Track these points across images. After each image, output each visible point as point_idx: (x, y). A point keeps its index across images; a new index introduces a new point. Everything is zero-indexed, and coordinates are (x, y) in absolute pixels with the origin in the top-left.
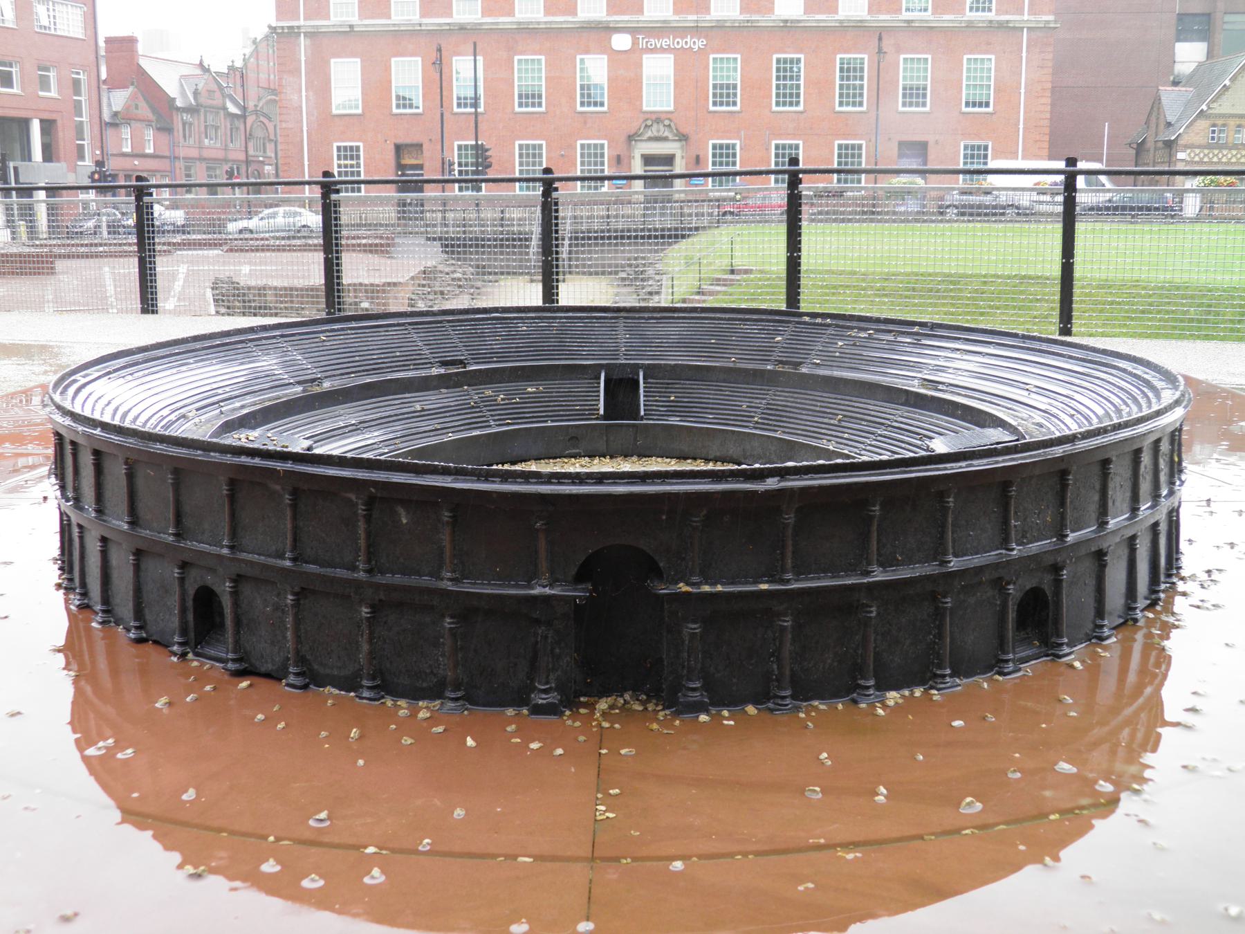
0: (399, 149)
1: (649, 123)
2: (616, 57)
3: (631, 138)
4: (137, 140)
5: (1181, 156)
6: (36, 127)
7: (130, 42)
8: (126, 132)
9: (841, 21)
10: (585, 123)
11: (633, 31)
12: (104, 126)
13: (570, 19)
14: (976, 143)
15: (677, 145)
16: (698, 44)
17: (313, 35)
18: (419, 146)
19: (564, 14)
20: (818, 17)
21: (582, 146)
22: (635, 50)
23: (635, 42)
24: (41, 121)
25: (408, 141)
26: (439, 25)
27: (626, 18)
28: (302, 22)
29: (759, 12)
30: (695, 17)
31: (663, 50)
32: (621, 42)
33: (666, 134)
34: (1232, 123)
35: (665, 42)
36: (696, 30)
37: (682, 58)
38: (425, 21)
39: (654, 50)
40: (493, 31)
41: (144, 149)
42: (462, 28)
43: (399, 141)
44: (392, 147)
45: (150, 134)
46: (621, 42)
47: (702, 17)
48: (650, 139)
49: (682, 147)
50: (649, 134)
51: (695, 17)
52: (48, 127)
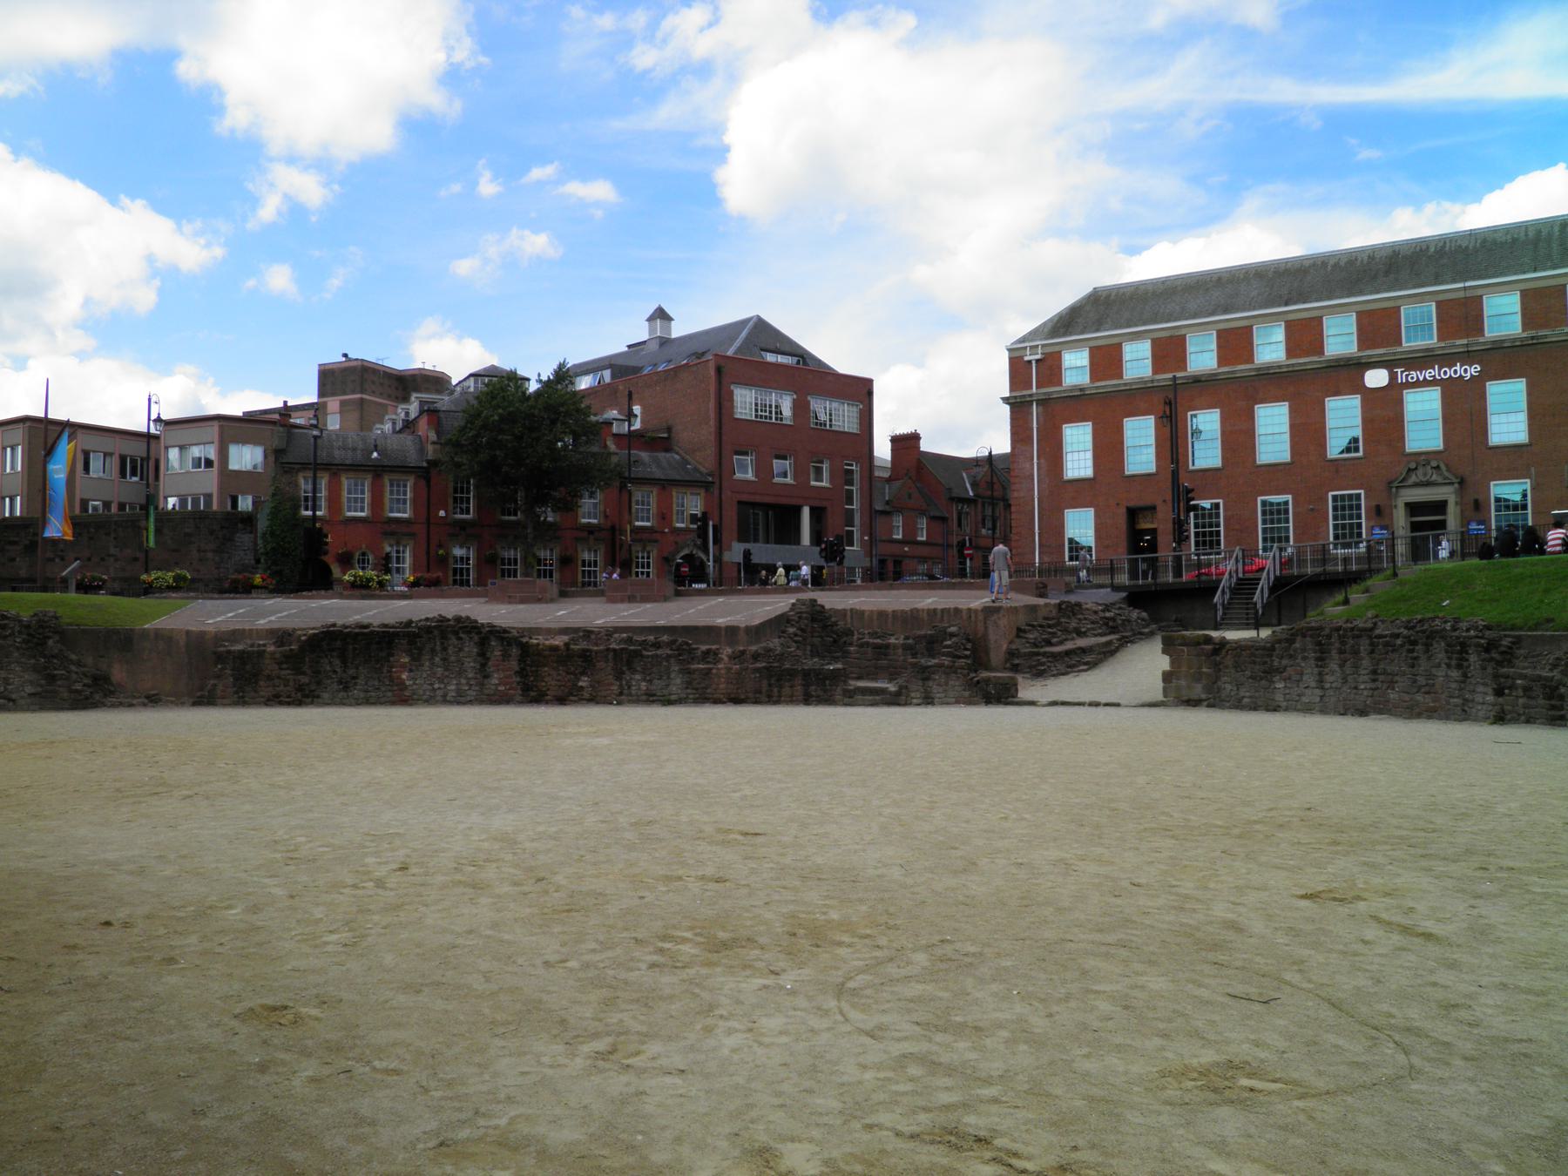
0: (1133, 514)
1: (1413, 466)
2: (1372, 398)
3: (1394, 485)
4: (910, 529)
6: (806, 513)
7: (914, 438)
8: (898, 521)
10: (1337, 471)
11: (1388, 364)
12: (872, 514)
13: (1316, 359)
16: (1474, 370)
17: (1044, 402)
18: (1153, 508)
19: (1308, 354)
21: (1335, 498)
23: (1393, 377)
24: (812, 510)
25: (1141, 504)
27: (1381, 351)
29: (1545, 326)
30: (1465, 341)
31: (1426, 383)
32: (1376, 378)
35: (1428, 374)
36: (1467, 357)
37: (1451, 389)
38: (1158, 377)
39: (1417, 384)
40: (1231, 380)
41: (915, 535)
42: (1197, 380)
43: (1132, 504)
44: (1122, 511)
45: (923, 523)
46: (1376, 378)
48: (1416, 485)
49: (1456, 492)
50: (1413, 479)
51: (1465, 341)
52: (817, 514)
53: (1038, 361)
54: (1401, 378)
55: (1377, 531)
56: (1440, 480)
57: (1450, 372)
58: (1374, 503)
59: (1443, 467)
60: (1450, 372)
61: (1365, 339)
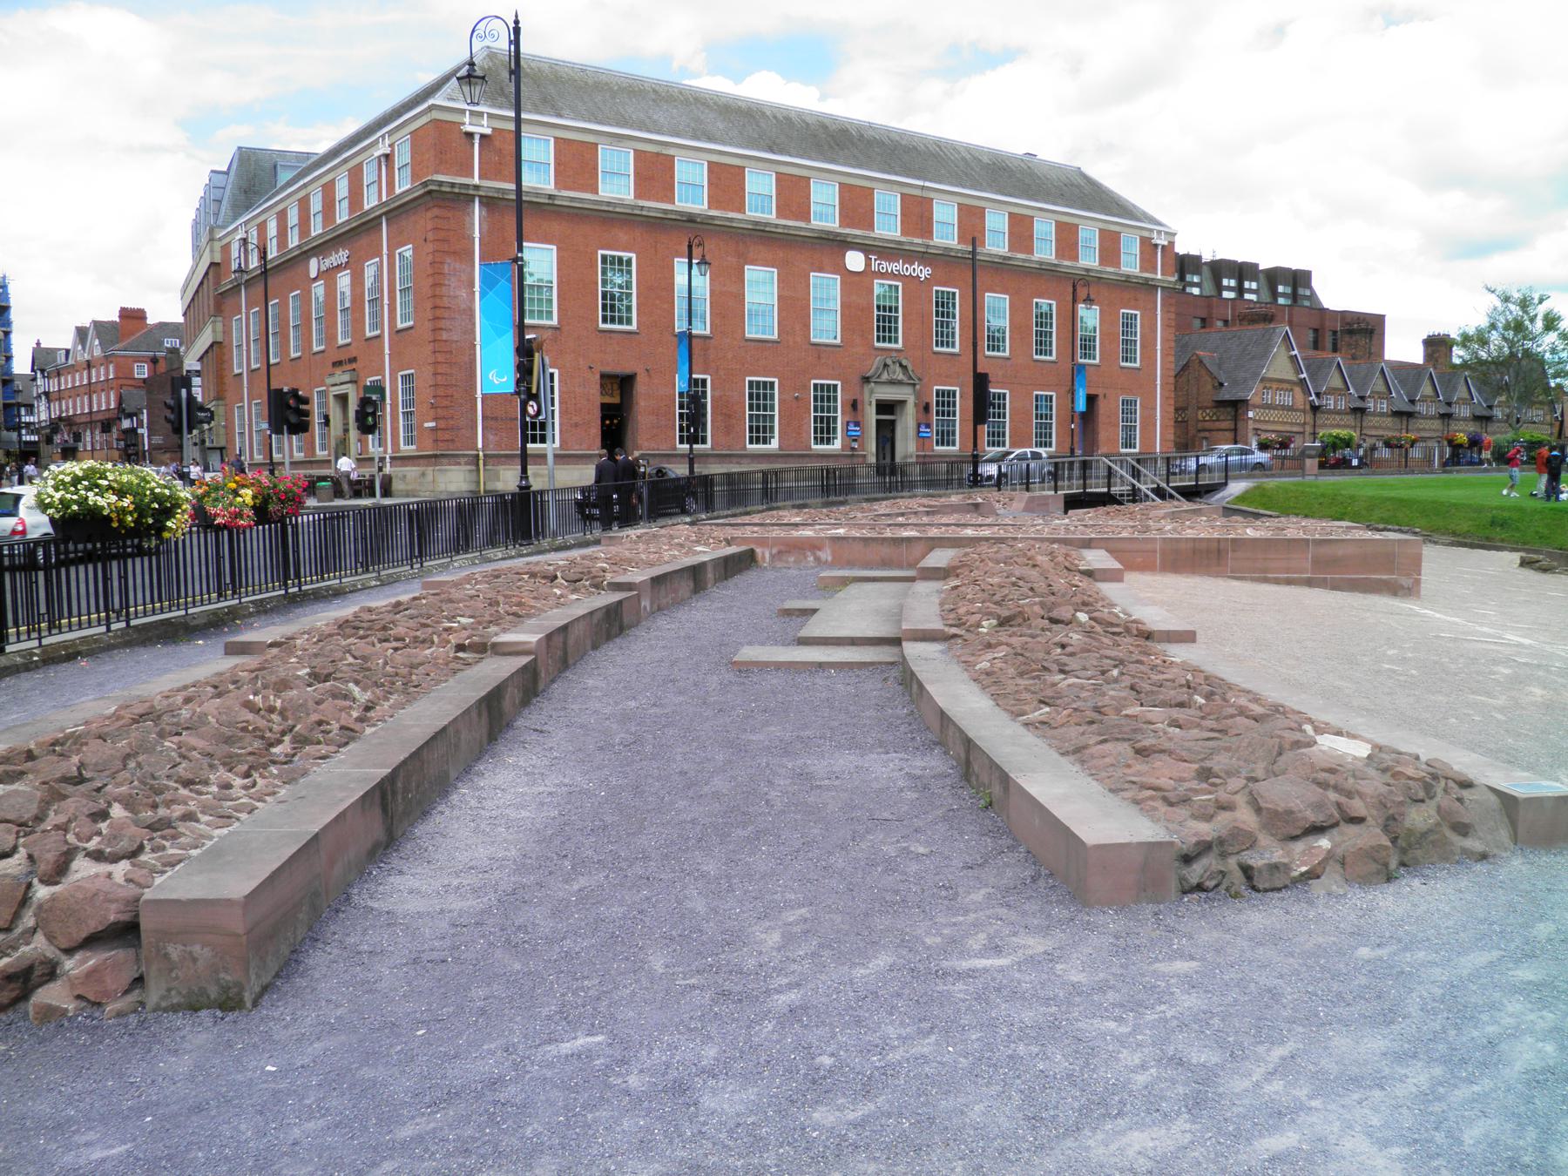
5: (1251, 414)
9: (1041, 263)
11: (866, 249)
14: (1129, 398)
15: (909, 390)
16: (923, 272)
20: (1020, 256)
22: (868, 274)
26: (665, 211)
28: (476, 180)
30: (919, 241)
31: (893, 276)
33: (901, 377)
34: (1275, 386)
36: (925, 257)
46: (855, 261)
47: (926, 241)
50: (885, 377)
53: (483, 136)
54: (874, 267)
55: (851, 427)
56: (905, 379)
57: (910, 270)
58: (851, 397)
59: (910, 368)
60: (910, 270)
61: (846, 218)
